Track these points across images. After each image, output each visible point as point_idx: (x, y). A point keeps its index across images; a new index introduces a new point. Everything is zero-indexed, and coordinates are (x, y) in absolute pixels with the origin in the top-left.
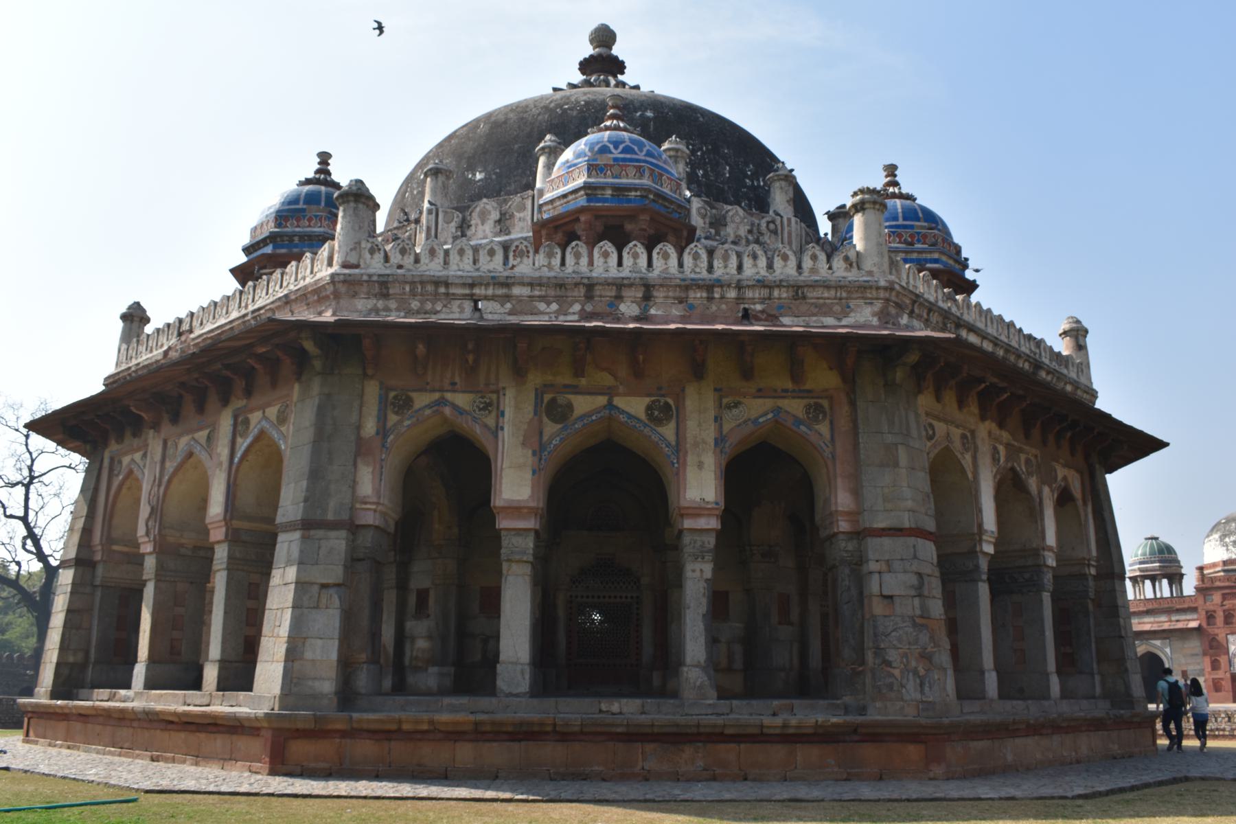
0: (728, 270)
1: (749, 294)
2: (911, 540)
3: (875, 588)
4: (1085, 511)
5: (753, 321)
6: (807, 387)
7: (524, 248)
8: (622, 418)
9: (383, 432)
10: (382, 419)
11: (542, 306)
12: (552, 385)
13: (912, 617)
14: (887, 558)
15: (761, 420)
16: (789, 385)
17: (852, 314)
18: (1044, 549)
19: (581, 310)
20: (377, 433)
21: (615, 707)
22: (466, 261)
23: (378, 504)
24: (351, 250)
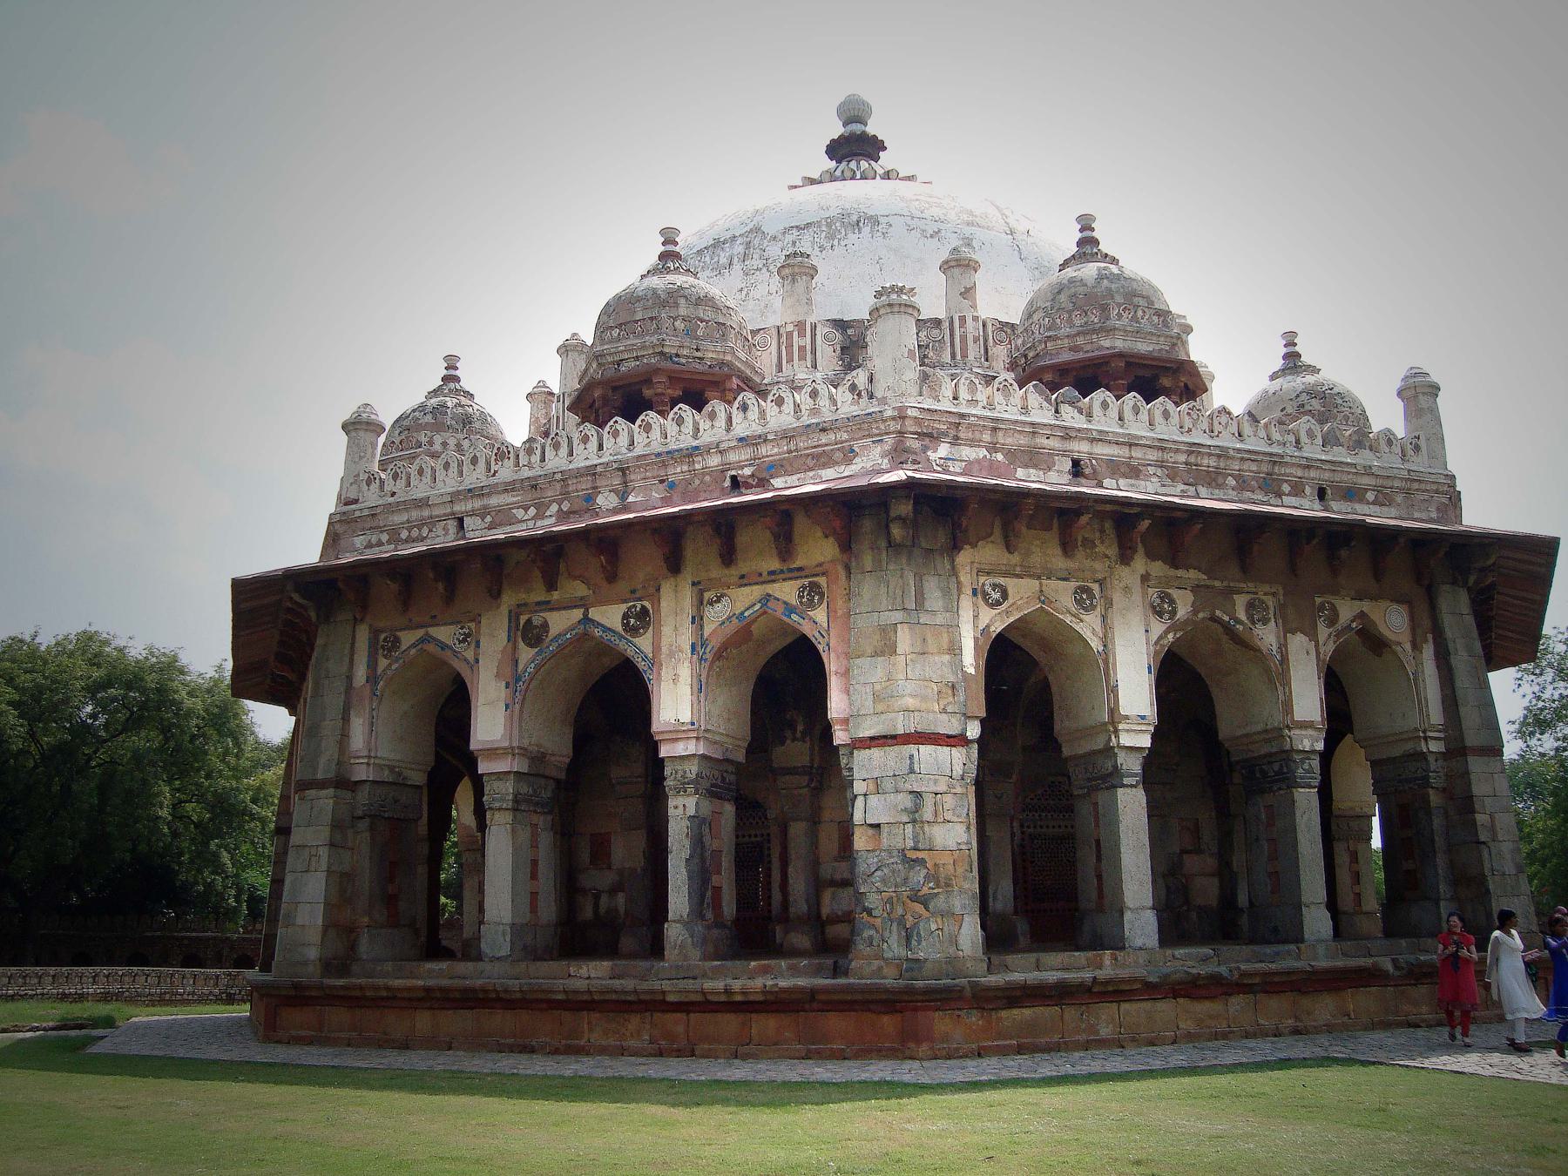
0: (682, 437)
1: (733, 457)
2: (912, 748)
3: (858, 817)
4: (1419, 664)
5: (743, 490)
6: (797, 564)
7: (505, 448)
8: (597, 632)
9: (372, 678)
10: (372, 665)
11: (520, 513)
12: (525, 605)
13: (903, 850)
14: (875, 777)
15: (746, 614)
16: (775, 564)
17: (857, 460)
18: (1290, 729)
19: (558, 511)
20: (367, 681)
21: (584, 971)
22: (478, 471)
23: (369, 757)
24: (351, 484)
